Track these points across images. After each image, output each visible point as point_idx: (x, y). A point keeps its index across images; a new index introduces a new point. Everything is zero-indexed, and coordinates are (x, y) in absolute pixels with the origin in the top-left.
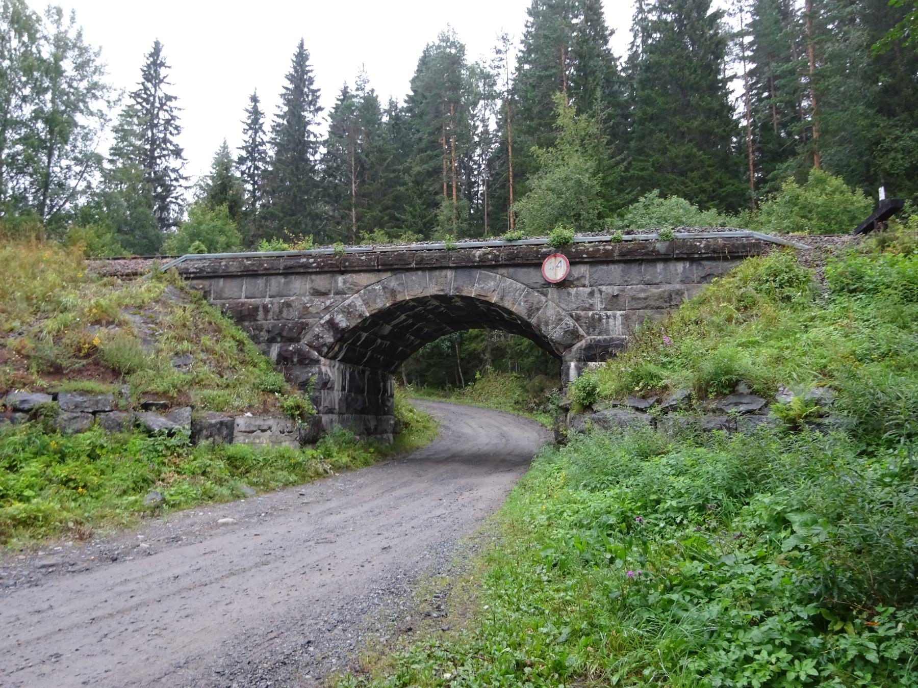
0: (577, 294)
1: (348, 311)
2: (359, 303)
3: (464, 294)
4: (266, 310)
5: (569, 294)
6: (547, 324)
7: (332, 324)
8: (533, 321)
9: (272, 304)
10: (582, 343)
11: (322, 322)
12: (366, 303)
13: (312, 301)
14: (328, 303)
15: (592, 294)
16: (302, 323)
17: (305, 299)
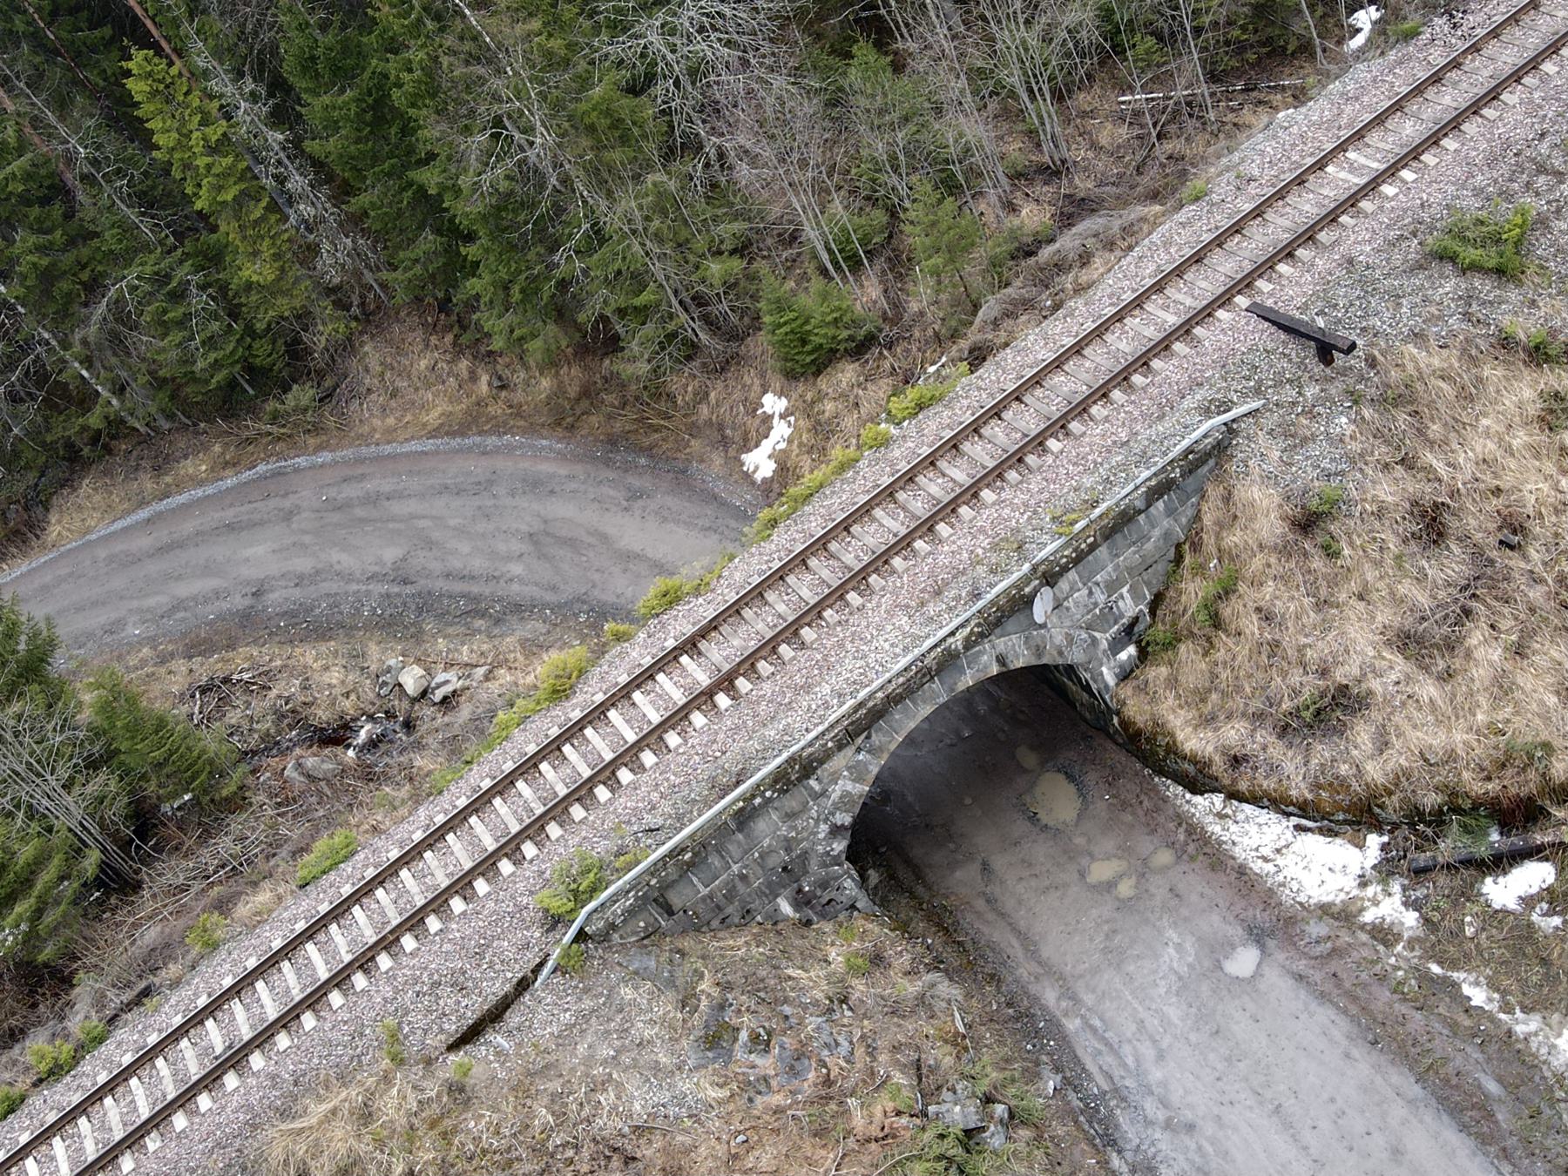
0: (1077, 603)
1: (845, 801)
2: (849, 786)
3: (961, 687)
4: (743, 878)
5: (1068, 609)
6: (1061, 653)
7: (836, 831)
8: (1045, 661)
9: (745, 867)
10: (1104, 645)
11: (821, 836)
12: (858, 779)
13: (794, 828)
14: (815, 815)
15: (1091, 593)
16: (798, 857)
17: (784, 831)
